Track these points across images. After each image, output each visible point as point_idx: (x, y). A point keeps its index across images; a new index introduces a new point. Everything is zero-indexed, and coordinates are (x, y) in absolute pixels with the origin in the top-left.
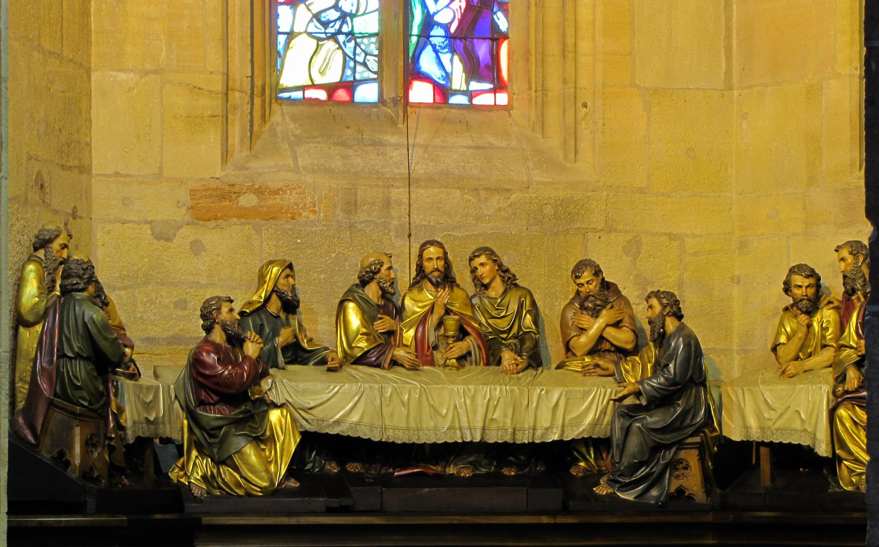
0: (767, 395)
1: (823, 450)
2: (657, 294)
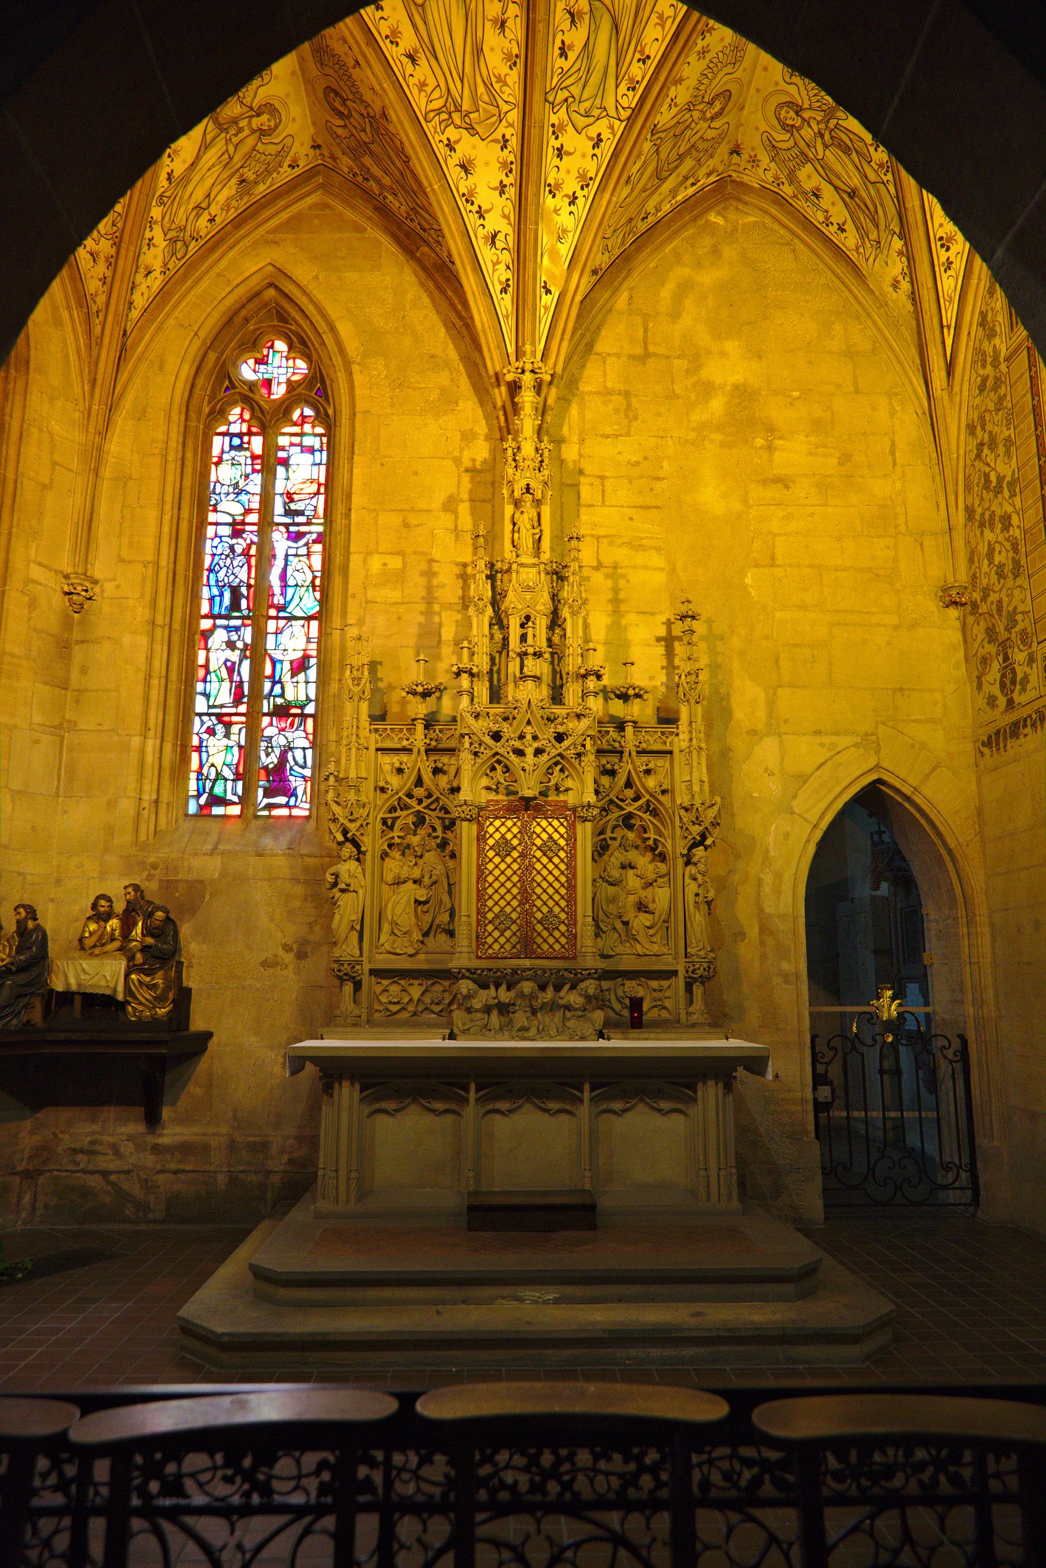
0: (85, 966)
1: (120, 997)
2: (23, 906)
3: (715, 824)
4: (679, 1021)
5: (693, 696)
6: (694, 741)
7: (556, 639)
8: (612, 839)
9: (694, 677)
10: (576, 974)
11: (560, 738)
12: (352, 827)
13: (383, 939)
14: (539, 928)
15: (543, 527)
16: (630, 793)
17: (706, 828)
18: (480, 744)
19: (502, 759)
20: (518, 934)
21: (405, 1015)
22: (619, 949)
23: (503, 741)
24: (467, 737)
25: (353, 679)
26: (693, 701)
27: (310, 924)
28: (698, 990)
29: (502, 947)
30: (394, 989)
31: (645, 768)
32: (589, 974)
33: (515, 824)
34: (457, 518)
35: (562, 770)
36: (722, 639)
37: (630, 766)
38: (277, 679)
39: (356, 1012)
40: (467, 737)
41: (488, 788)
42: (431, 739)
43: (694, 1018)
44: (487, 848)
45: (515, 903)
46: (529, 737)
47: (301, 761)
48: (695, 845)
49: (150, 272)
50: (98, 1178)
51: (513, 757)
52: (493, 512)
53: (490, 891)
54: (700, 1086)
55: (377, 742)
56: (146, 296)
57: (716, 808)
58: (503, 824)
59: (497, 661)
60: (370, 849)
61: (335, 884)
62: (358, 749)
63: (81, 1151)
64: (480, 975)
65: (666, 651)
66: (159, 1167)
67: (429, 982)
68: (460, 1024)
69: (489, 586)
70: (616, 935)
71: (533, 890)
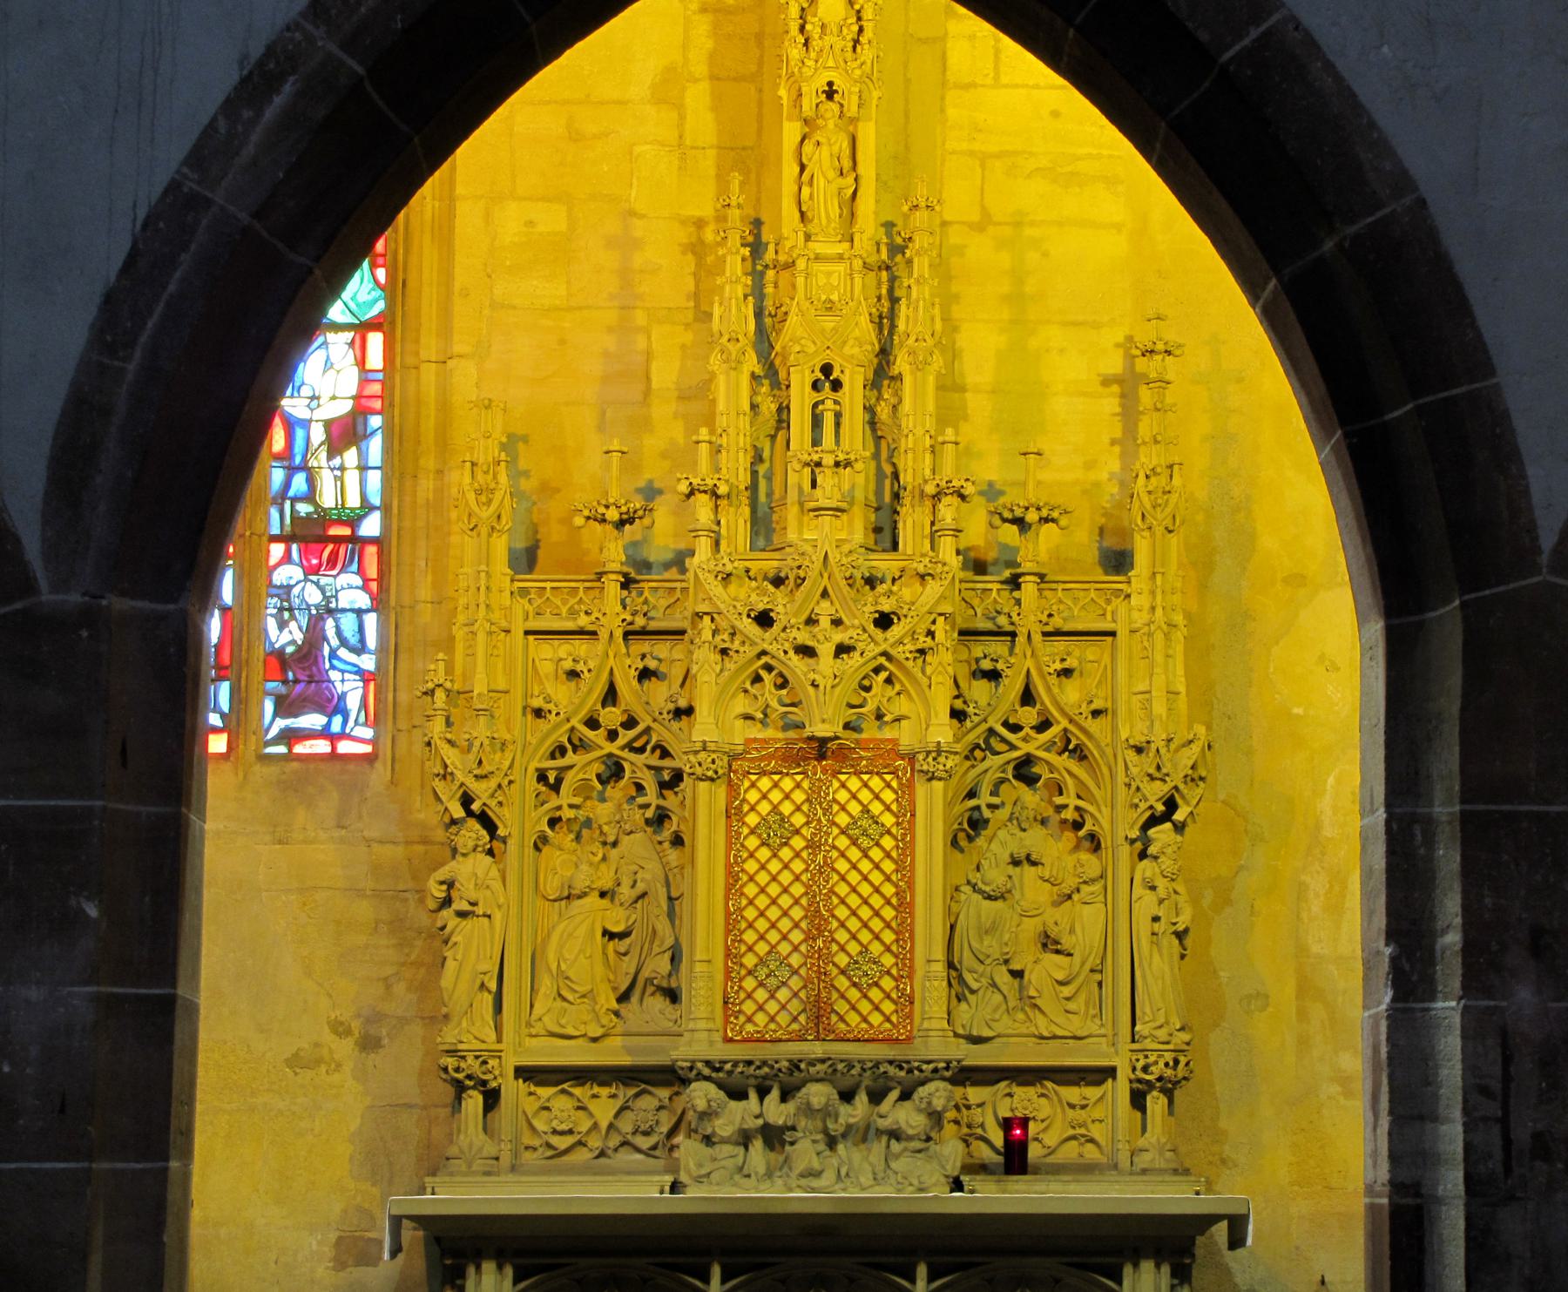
3: (1193, 779)
4: (1115, 1167)
5: (1160, 518)
6: (1159, 612)
7: (883, 412)
8: (992, 807)
9: (1163, 480)
10: (910, 1071)
11: (884, 621)
12: (481, 790)
13: (538, 1010)
14: (842, 982)
15: (861, 169)
16: (1028, 716)
17: (1176, 788)
18: (733, 634)
19: (773, 662)
20: (802, 994)
21: (582, 1156)
22: (1004, 1025)
23: (776, 628)
24: (707, 619)
25: (479, 492)
26: (1159, 530)
27: (386, 979)
28: (1156, 1103)
29: (772, 1019)
30: (562, 1104)
31: (1058, 666)
32: (935, 1070)
33: (798, 785)
34: (682, 117)
35: (889, 681)
36: (1240, 380)
37: (1029, 663)
38: (298, 460)
39: (490, 1149)
40: (707, 619)
41: (748, 717)
42: (634, 614)
43: (1144, 1160)
44: (745, 831)
45: (796, 937)
46: (825, 622)
47: (353, 640)
48: (1153, 821)
51: (795, 660)
52: (760, 104)
53: (750, 913)
54: (1128, 1270)
55: (527, 618)
57: (1196, 748)
58: (776, 785)
59: (766, 454)
60: (515, 832)
61: (447, 902)
62: (490, 633)
64: (730, 1073)
65: (1123, 406)
67: (632, 1092)
68: (692, 1165)
69: (750, 311)
70: (998, 998)
71: (830, 911)
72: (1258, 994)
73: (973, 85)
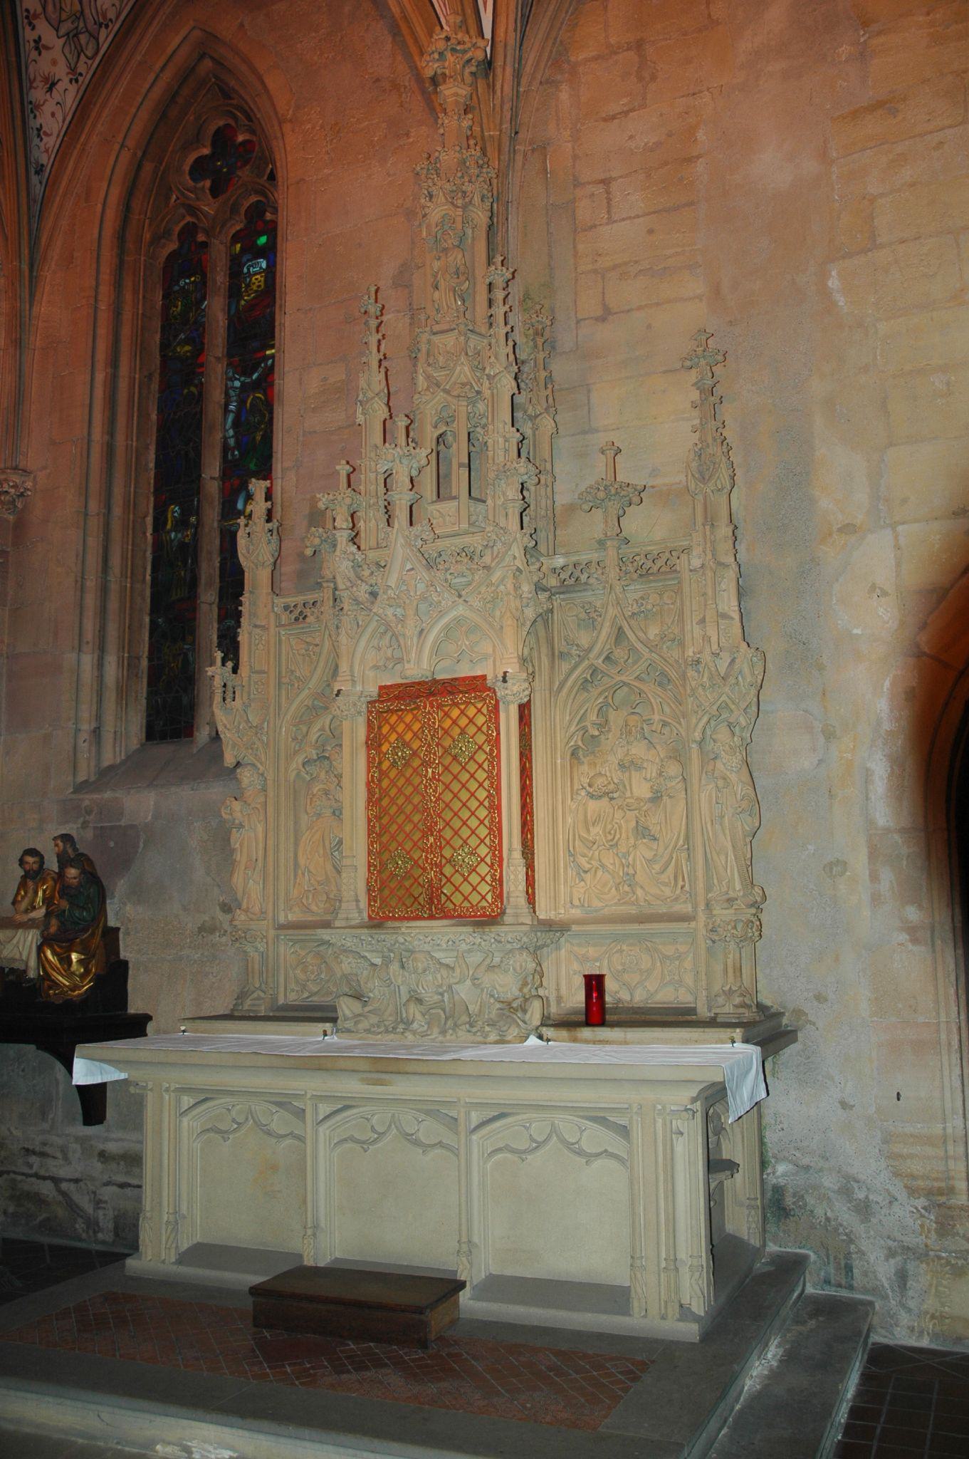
49: (53, 84)
50: (49, 1184)
56: (60, 117)
63: (34, 1153)
66: (106, 1178)
72: (838, 861)
73: (595, 226)
